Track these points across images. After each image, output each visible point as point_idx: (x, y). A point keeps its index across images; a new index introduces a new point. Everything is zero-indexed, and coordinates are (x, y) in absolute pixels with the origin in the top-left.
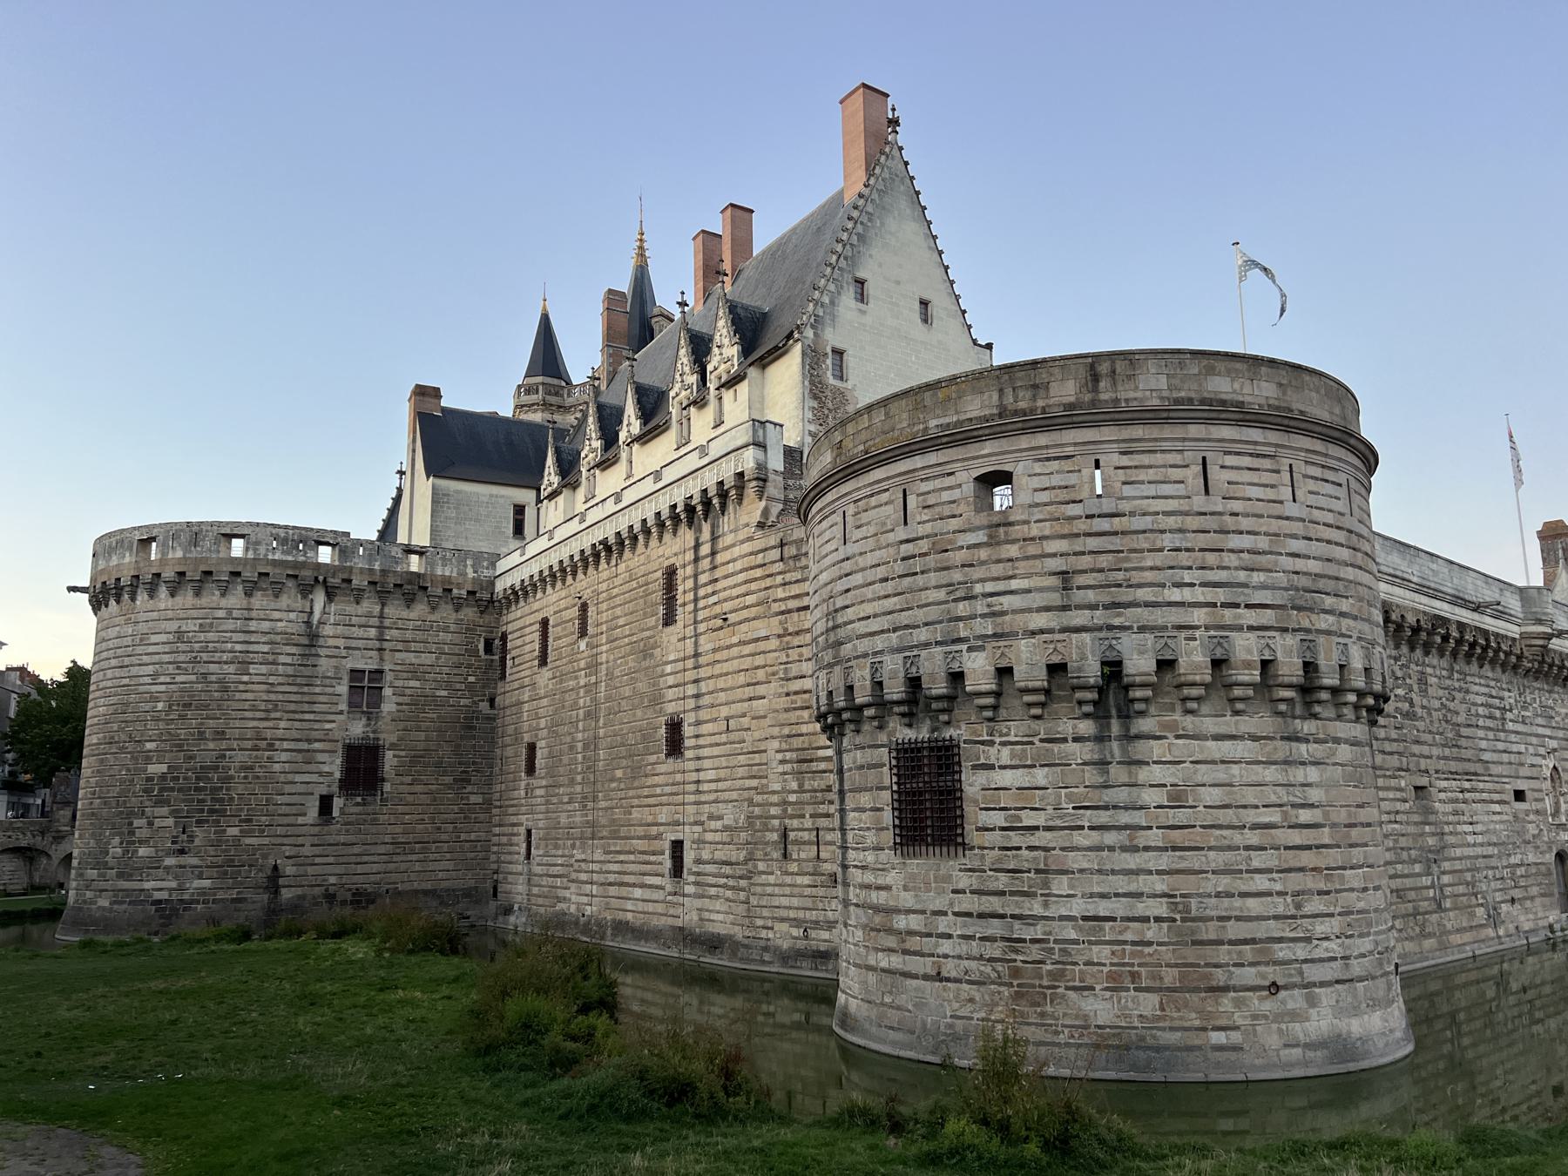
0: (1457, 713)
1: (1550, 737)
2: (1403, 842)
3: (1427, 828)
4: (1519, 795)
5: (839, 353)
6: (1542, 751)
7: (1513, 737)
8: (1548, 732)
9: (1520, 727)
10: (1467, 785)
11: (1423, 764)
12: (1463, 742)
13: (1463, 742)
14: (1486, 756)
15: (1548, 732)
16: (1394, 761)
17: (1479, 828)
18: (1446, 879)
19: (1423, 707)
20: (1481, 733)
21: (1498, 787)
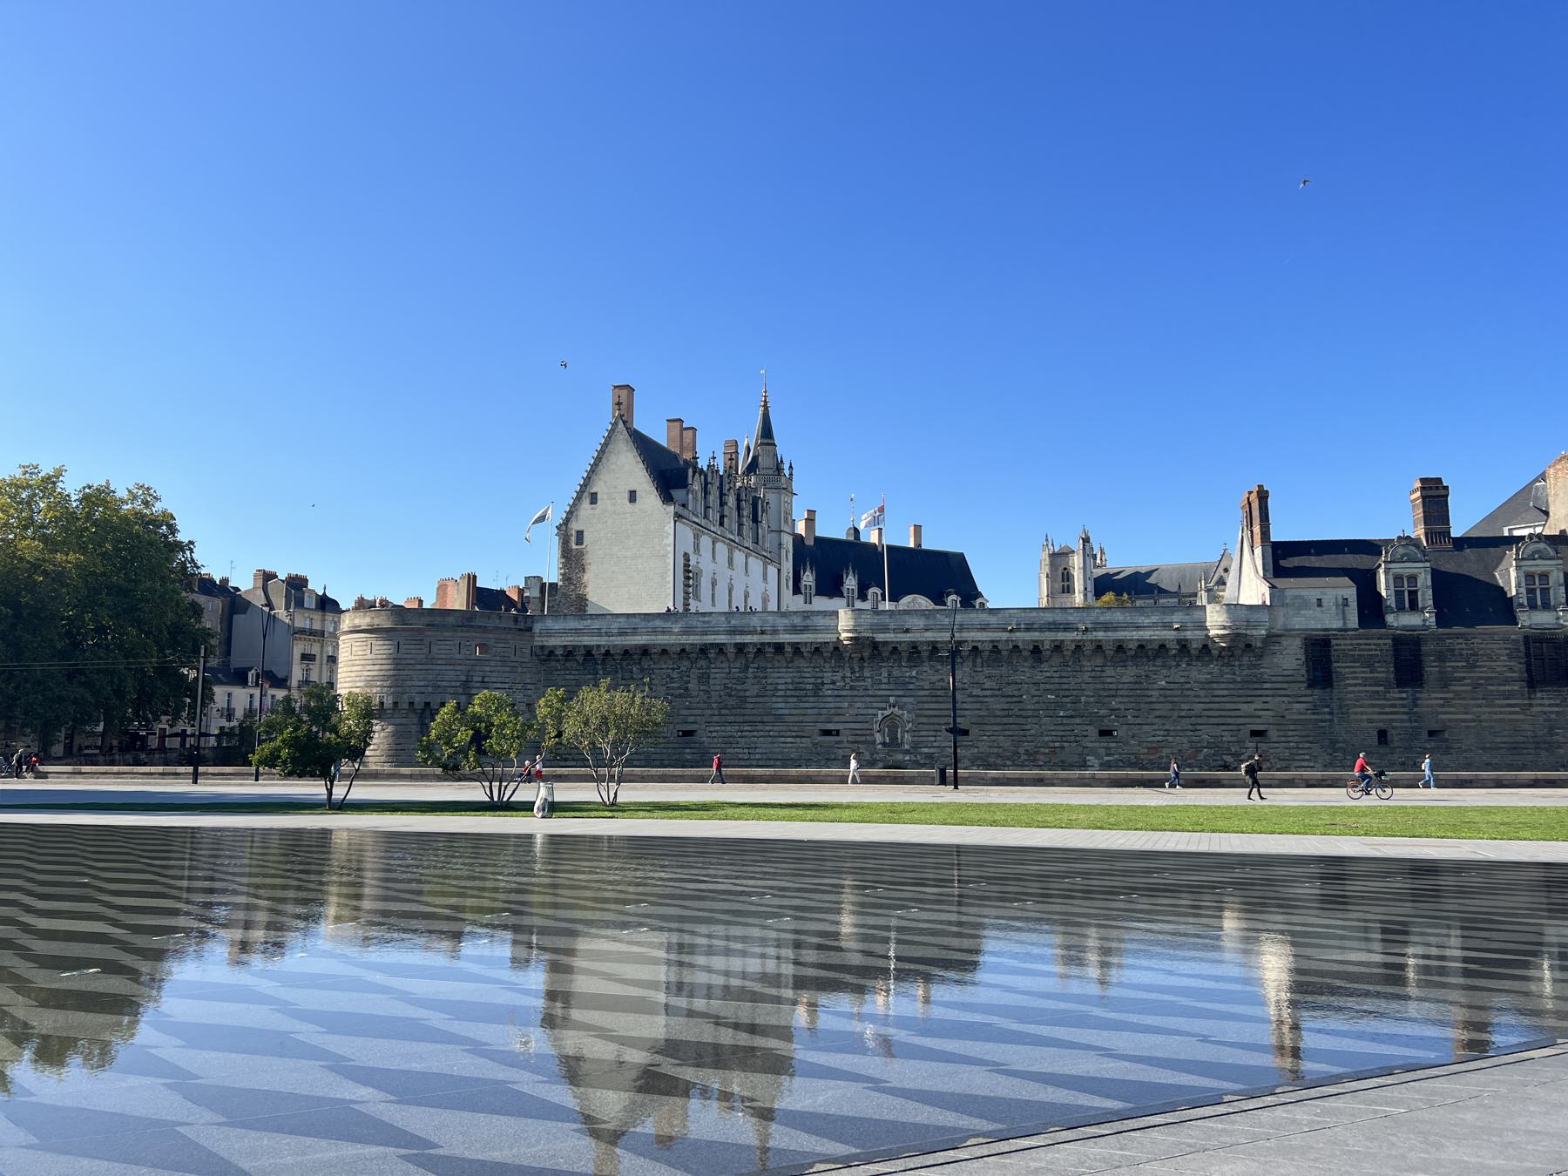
2: (658, 757)
3: (688, 751)
5: (580, 534)
6: (883, 705)
7: (830, 699)
8: (901, 693)
11: (691, 719)
13: (748, 706)
14: (781, 712)
15: (901, 693)
20: (780, 700)
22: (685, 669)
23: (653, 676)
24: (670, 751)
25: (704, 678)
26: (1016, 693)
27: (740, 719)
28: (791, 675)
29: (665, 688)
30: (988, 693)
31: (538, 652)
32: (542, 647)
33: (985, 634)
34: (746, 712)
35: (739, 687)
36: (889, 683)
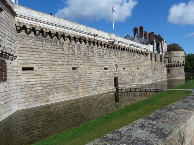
0: (89, 54)
1: (116, 59)
2: (67, 78)
3: (76, 75)
4: (106, 69)
6: (114, 61)
7: (106, 59)
8: (116, 58)
9: (108, 57)
10: (90, 67)
11: (76, 63)
12: (90, 60)
13: (90, 60)
15: (116, 58)
16: (66, 63)
17: (93, 74)
18: (80, 84)
19: (78, 53)
20: (97, 58)
21: (100, 67)
22: (73, 44)
23: (64, 46)
24: (71, 75)
25: (79, 49)
26: (129, 60)
27: (88, 64)
28: (98, 51)
29: (68, 51)
30: (127, 59)
31: (17, 25)
32: (19, 23)
33: (127, 45)
34: (90, 61)
35: (88, 53)
36: (114, 55)
